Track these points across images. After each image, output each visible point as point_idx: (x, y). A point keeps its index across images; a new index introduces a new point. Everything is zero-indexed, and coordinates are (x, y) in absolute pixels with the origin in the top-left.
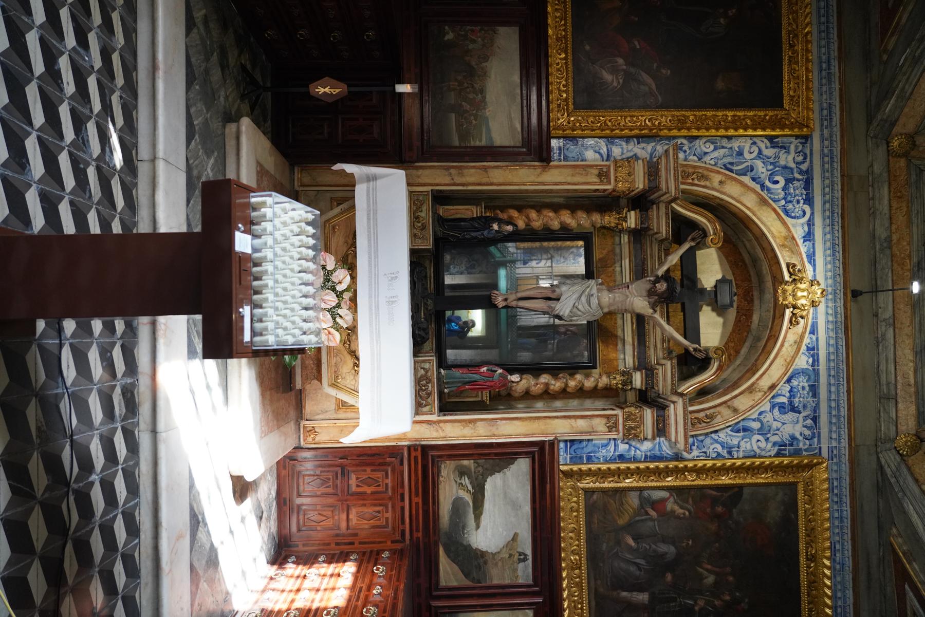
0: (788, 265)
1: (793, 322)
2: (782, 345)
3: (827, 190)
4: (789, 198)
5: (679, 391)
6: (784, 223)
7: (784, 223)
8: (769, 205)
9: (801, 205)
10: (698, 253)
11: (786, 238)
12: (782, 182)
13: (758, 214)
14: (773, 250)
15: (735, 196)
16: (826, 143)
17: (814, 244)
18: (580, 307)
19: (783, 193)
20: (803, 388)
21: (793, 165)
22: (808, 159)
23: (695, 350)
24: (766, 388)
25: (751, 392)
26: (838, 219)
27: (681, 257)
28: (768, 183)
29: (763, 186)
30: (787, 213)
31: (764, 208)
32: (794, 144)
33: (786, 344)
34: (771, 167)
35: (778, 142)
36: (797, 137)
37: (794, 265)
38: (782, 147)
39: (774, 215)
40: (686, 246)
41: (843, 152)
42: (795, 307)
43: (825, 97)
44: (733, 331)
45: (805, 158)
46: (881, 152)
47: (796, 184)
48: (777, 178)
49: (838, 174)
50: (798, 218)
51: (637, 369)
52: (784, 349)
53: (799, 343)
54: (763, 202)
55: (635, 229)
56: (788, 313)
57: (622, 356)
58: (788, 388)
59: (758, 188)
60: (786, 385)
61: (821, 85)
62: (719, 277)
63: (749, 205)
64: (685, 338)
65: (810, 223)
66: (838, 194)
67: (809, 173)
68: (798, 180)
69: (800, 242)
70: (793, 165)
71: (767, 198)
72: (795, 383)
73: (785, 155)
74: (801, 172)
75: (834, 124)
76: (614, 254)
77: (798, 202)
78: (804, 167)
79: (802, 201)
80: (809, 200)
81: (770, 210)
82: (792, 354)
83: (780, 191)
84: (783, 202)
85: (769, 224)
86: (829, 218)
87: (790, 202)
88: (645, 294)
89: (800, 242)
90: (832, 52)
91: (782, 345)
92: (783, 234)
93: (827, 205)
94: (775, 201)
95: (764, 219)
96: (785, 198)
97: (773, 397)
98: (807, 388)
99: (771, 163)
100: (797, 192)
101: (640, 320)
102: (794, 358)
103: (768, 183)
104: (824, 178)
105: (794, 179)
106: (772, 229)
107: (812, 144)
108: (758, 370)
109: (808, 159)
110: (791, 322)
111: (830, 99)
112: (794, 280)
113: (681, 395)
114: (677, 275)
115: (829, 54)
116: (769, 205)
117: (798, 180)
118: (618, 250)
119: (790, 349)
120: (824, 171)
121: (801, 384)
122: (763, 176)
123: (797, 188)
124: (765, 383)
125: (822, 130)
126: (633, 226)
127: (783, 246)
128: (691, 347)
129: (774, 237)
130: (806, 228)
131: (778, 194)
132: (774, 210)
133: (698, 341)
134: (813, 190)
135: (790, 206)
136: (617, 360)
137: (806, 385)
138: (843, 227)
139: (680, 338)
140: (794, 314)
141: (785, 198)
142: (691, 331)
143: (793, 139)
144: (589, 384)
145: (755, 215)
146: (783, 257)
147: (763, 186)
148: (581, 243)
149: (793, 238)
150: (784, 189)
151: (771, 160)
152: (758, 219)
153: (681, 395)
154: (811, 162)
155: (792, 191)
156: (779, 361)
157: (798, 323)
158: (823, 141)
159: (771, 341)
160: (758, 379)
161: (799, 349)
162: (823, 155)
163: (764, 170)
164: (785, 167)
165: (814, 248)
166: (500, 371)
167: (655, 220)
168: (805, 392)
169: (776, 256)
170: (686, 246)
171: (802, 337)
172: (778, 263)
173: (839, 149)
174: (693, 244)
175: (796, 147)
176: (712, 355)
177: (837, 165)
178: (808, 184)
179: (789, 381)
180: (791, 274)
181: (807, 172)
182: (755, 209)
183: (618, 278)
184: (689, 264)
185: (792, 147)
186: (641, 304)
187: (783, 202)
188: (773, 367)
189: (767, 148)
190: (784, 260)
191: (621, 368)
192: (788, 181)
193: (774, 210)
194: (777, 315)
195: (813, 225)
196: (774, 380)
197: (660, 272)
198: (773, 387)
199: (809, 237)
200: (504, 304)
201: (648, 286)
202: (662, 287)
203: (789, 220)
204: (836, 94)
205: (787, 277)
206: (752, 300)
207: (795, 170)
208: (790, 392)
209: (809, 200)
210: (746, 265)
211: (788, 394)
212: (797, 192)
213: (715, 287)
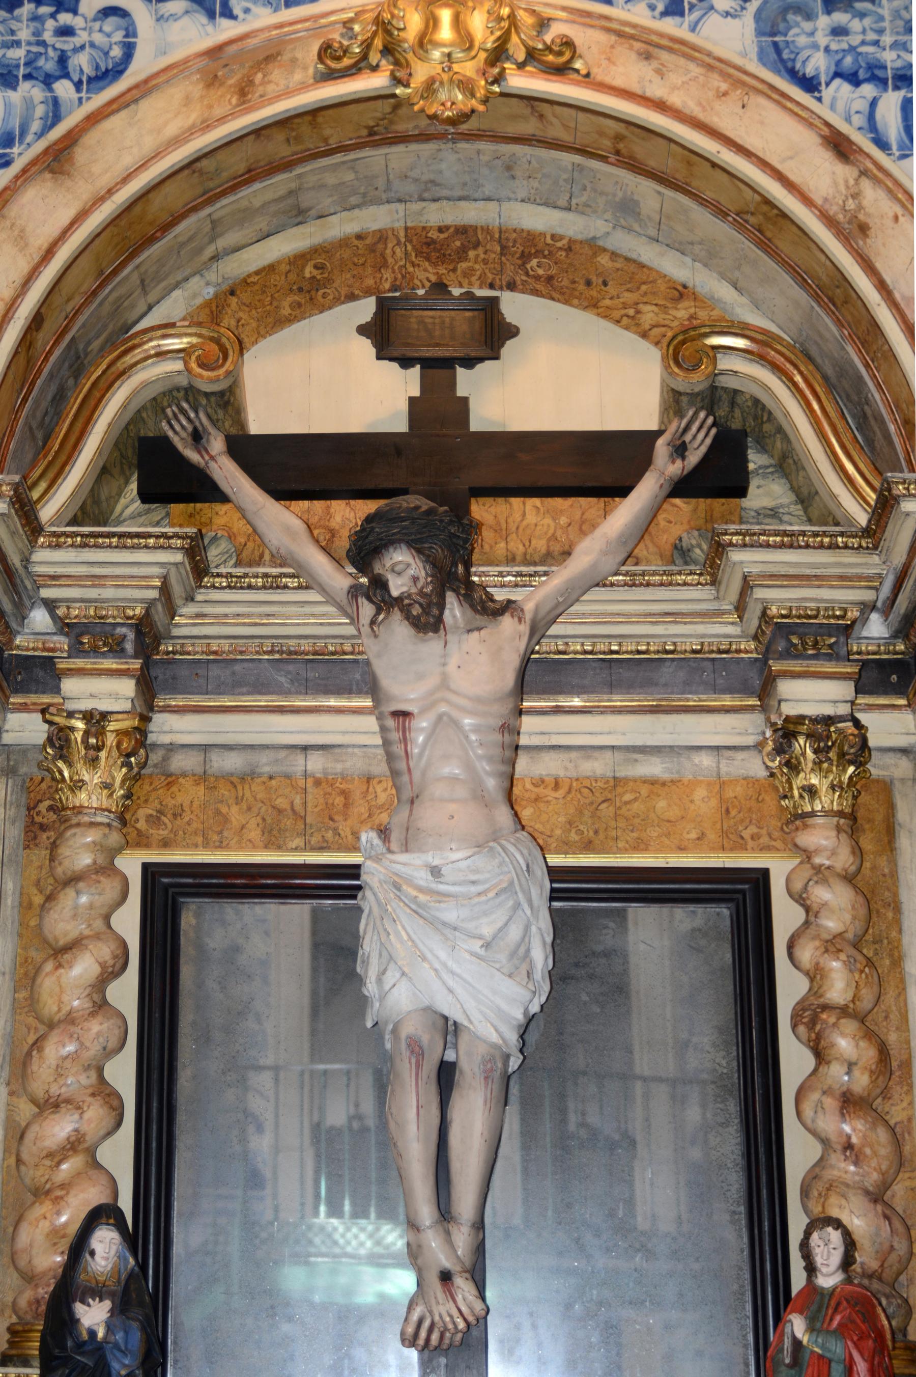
0: (330, 76)
1: (560, 61)
2: (661, 106)
4: (49, 65)
5: (862, 518)
7: (145, 88)
8: (71, 139)
9: (77, 22)
10: (255, 427)
11: (212, 81)
13: (105, 181)
14: (258, 132)
15: (24, 266)
18: (487, 931)
19: (25, 87)
20: (839, 31)
23: (680, 450)
24: (844, 172)
25: (864, 229)
27: (282, 494)
30: (106, 75)
31: (81, 155)
33: (656, 90)
37: (326, 51)
40: (227, 473)
42: (498, 54)
44: (592, 305)
50: (131, 32)
51: (765, 690)
52: (676, 99)
53: (649, 46)
54: (57, 160)
55: (138, 683)
56: (521, 81)
57: (706, 761)
58: (842, 88)
60: (827, 93)
62: (366, 347)
63: (65, 216)
64: (623, 491)
69: (226, 30)
71: (40, 146)
72: (817, 64)
76: (248, 776)
77: (66, 32)
79: (65, 18)
81: (91, 138)
82: (695, 70)
85: (149, 144)
87: (63, 60)
88: (432, 645)
91: (661, 106)
92: (197, 90)
94: (55, 113)
95: (128, 160)
96: (48, 81)
97: (882, 144)
98: (840, 18)
100: (24, 34)
101: (539, 675)
102: (714, 64)
106: (172, 130)
108: (767, 202)
110: (561, 71)
112: (387, 51)
113: (885, 506)
114: (347, 515)
116: (71, 139)
118: (232, 762)
119: (675, 78)
121: (822, 39)
124: (823, 174)
126: (128, 687)
127: (244, 91)
128: (665, 467)
129: (206, 126)
131: (29, 104)
132: (94, 119)
133: (647, 439)
135: (82, 62)
136: (721, 784)
137: (824, 22)
139: (625, 513)
140: (532, 55)
141: (48, 81)
142: (595, 466)
144: (838, 906)
145: (110, 192)
146: (288, 93)
148: (188, 920)
149: (215, 52)
152: (126, 180)
153: (885, 506)
155: (18, 54)
156: (726, 118)
157: (568, 43)
159: (640, 148)
160: (807, 200)
161: (678, 46)
166: (797, 1325)
167: (108, 593)
168: (856, 25)
169: (284, 123)
170: (227, 473)
171: (624, 34)
172: (314, 113)
174: (217, 444)
176: (696, 381)
179: (810, 85)
180: (361, 66)
182: (83, 191)
183: (354, 764)
184: (300, 467)
186: (468, 665)
187: (64, 89)
188: (752, 142)
190: (303, 88)
191: (755, 767)
193: (94, 119)
194: (529, 127)
196: (809, 141)
197: (340, 579)
198: (839, 146)
200: (464, 1287)
201: (398, 629)
202: (404, 569)
203: (142, 65)
205: (374, 82)
206: (462, 231)
208: (854, 80)
210: (315, 251)
211: (868, 90)
212: (24, 34)
213: (405, 363)
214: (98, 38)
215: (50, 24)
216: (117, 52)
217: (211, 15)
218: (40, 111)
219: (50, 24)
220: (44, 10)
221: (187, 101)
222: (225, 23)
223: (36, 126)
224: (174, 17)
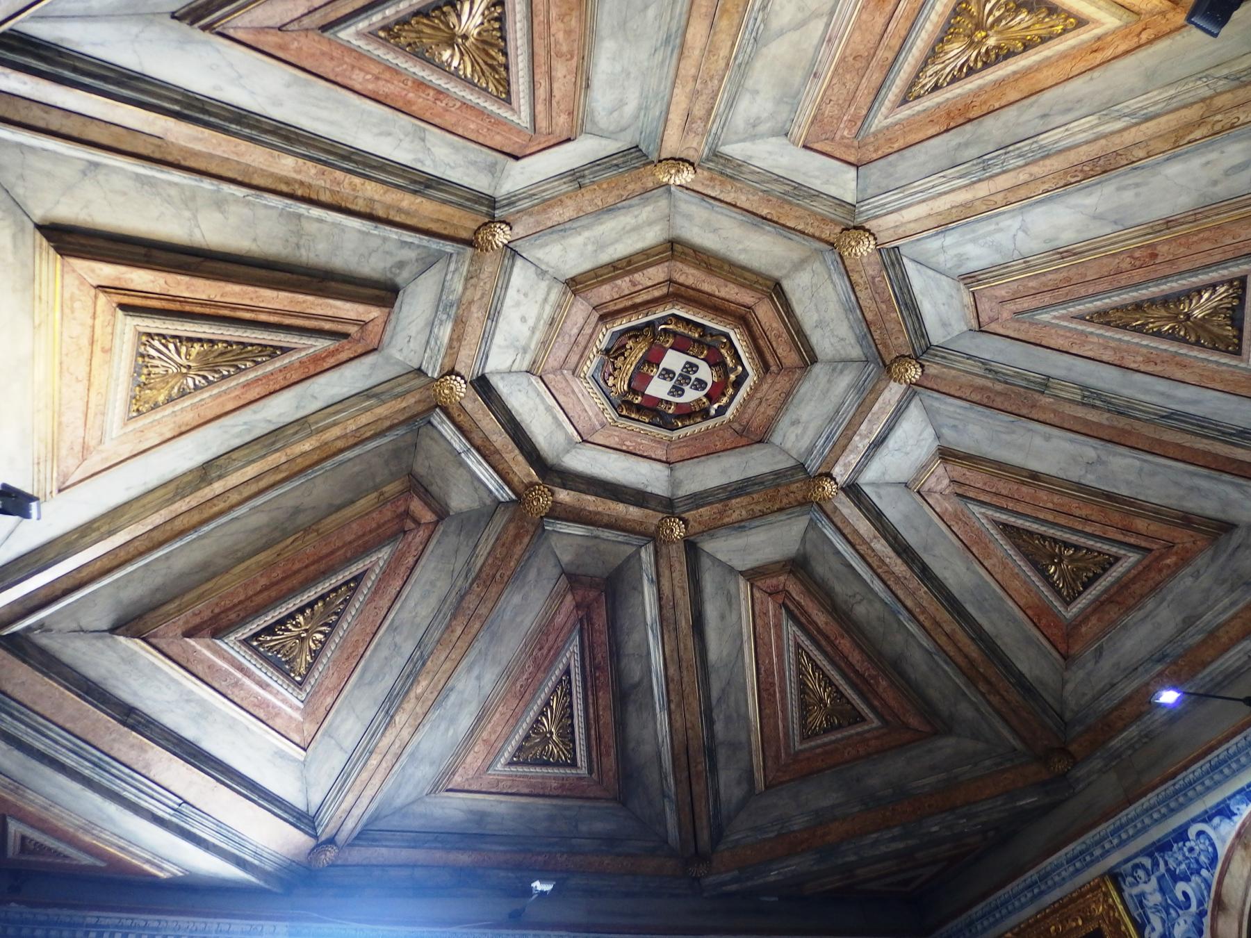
3: (1156, 816)
4: (1194, 866)
6: (1228, 859)
7: (1228, 859)
9: (1193, 844)
12: (1181, 886)
13: (1239, 905)
16: (1107, 846)
17: (1230, 798)
19: (1193, 878)
21: (1154, 880)
22: (1137, 861)
26: (1180, 781)
28: (1194, 908)
29: (1202, 914)
30: (1214, 859)
31: (1226, 899)
32: (1130, 891)
34: (1172, 911)
35: (1139, 915)
36: (1120, 891)
38: (1142, 907)
39: (1227, 880)
41: (1106, 817)
43: (1064, 874)
45: (1136, 867)
46: (1081, 772)
47: (1172, 865)
48: (1181, 897)
49: (1131, 811)
50: (1210, 839)
54: (1219, 904)
59: (1207, 921)
61: (1056, 885)
65: (1207, 817)
66: (1151, 798)
67: (1149, 852)
68: (1166, 863)
69: (1238, 821)
70: (1154, 880)
73: (1149, 897)
74: (1156, 864)
75: (1084, 847)
77: (1191, 850)
78: (1147, 862)
79: (1188, 844)
80: (1181, 835)
81: (1224, 891)
83: (1193, 884)
84: (1204, 872)
86: (1185, 795)
87: (1197, 861)
89: (1238, 821)
90: (1021, 887)
92: (1243, 853)
93: (1173, 805)
94: (1209, 887)
99: (1168, 914)
100: (1180, 858)
103: (1194, 908)
104: (1145, 829)
105: (1168, 870)
107: (1119, 865)
109: (1137, 861)
111: (1062, 865)
115: (1022, 891)
117: (1166, 863)
120: (1139, 832)
122: (1190, 920)
123: (1176, 859)
125: (1097, 860)
130: (1216, 820)
131: (1197, 884)
134: (1167, 835)
135: (1203, 859)
138: (1185, 768)
141: (1198, 873)
143: (1126, 895)
147: (1202, 914)
149: (1239, 835)
150: (1187, 880)
151: (1164, 915)
154: (1136, 855)
155: (1183, 866)
158: (1108, 851)
162: (1122, 843)
163: (1181, 921)
164: (1162, 890)
165: (1234, 795)
173: (1104, 825)
175: (1132, 885)
177: (1123, 817)
178: (1163, 847)
181: (1151, 855)
182: (1234, 913)
185: (1135, 891)
187: (1204, 872)
189: (1153, 929)
192: (1176, 878)
195: (1206, 812)
199: (1224, 811)
203: (1222, 852)
204: (1053, 859)
207: (1158, 874)
209: (1181, 835)
212: (1180, 858)
214: (1202, 847)
215: (1185, 849)
216: (1210, 849)
217: (1230, 818)
218: (1203, 886)
219: (1185, 849)
220: (1181, 844)
221: (1243, 860)
222: (1235, 818)
223: (1205, 893)
224: (1219, 825)
